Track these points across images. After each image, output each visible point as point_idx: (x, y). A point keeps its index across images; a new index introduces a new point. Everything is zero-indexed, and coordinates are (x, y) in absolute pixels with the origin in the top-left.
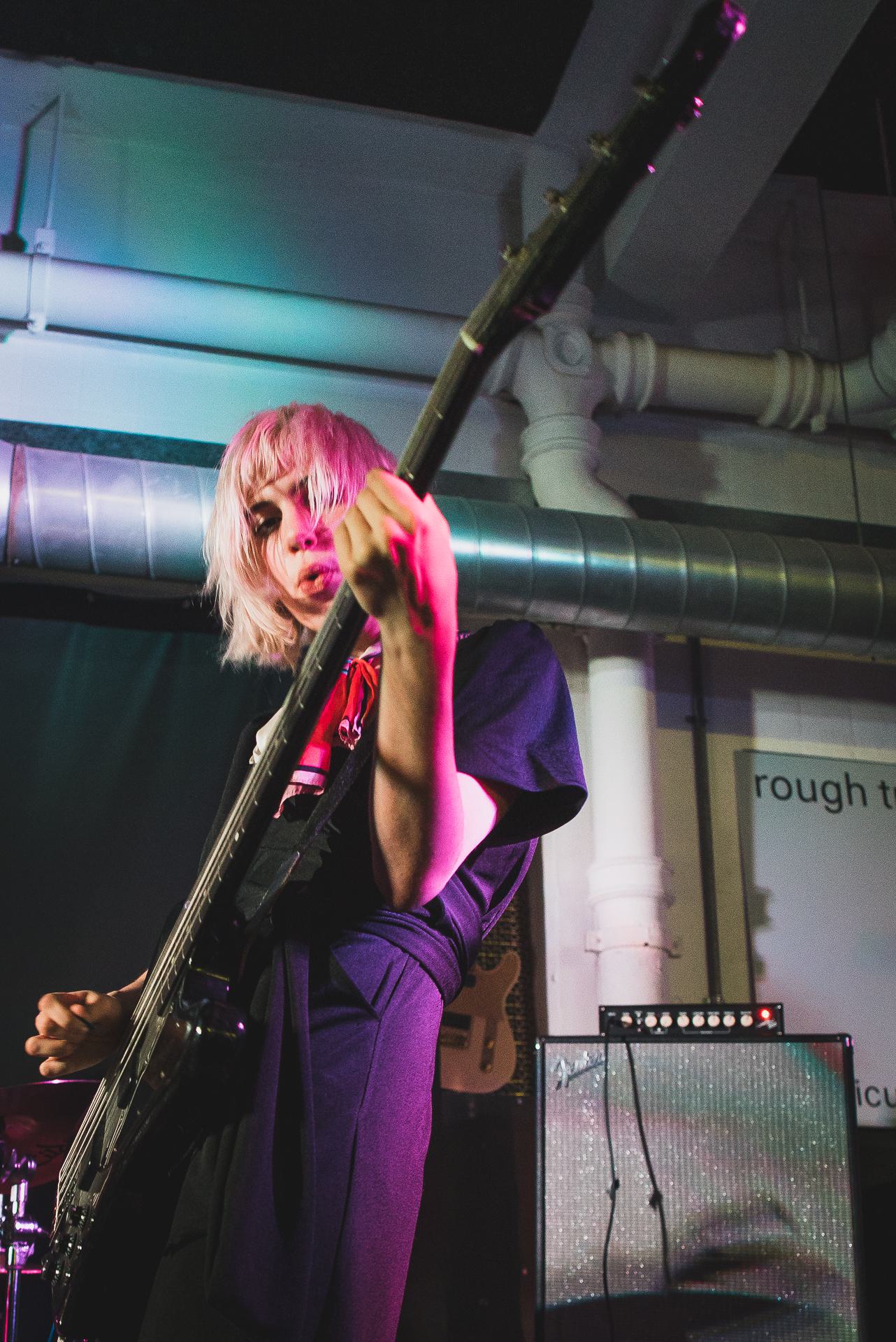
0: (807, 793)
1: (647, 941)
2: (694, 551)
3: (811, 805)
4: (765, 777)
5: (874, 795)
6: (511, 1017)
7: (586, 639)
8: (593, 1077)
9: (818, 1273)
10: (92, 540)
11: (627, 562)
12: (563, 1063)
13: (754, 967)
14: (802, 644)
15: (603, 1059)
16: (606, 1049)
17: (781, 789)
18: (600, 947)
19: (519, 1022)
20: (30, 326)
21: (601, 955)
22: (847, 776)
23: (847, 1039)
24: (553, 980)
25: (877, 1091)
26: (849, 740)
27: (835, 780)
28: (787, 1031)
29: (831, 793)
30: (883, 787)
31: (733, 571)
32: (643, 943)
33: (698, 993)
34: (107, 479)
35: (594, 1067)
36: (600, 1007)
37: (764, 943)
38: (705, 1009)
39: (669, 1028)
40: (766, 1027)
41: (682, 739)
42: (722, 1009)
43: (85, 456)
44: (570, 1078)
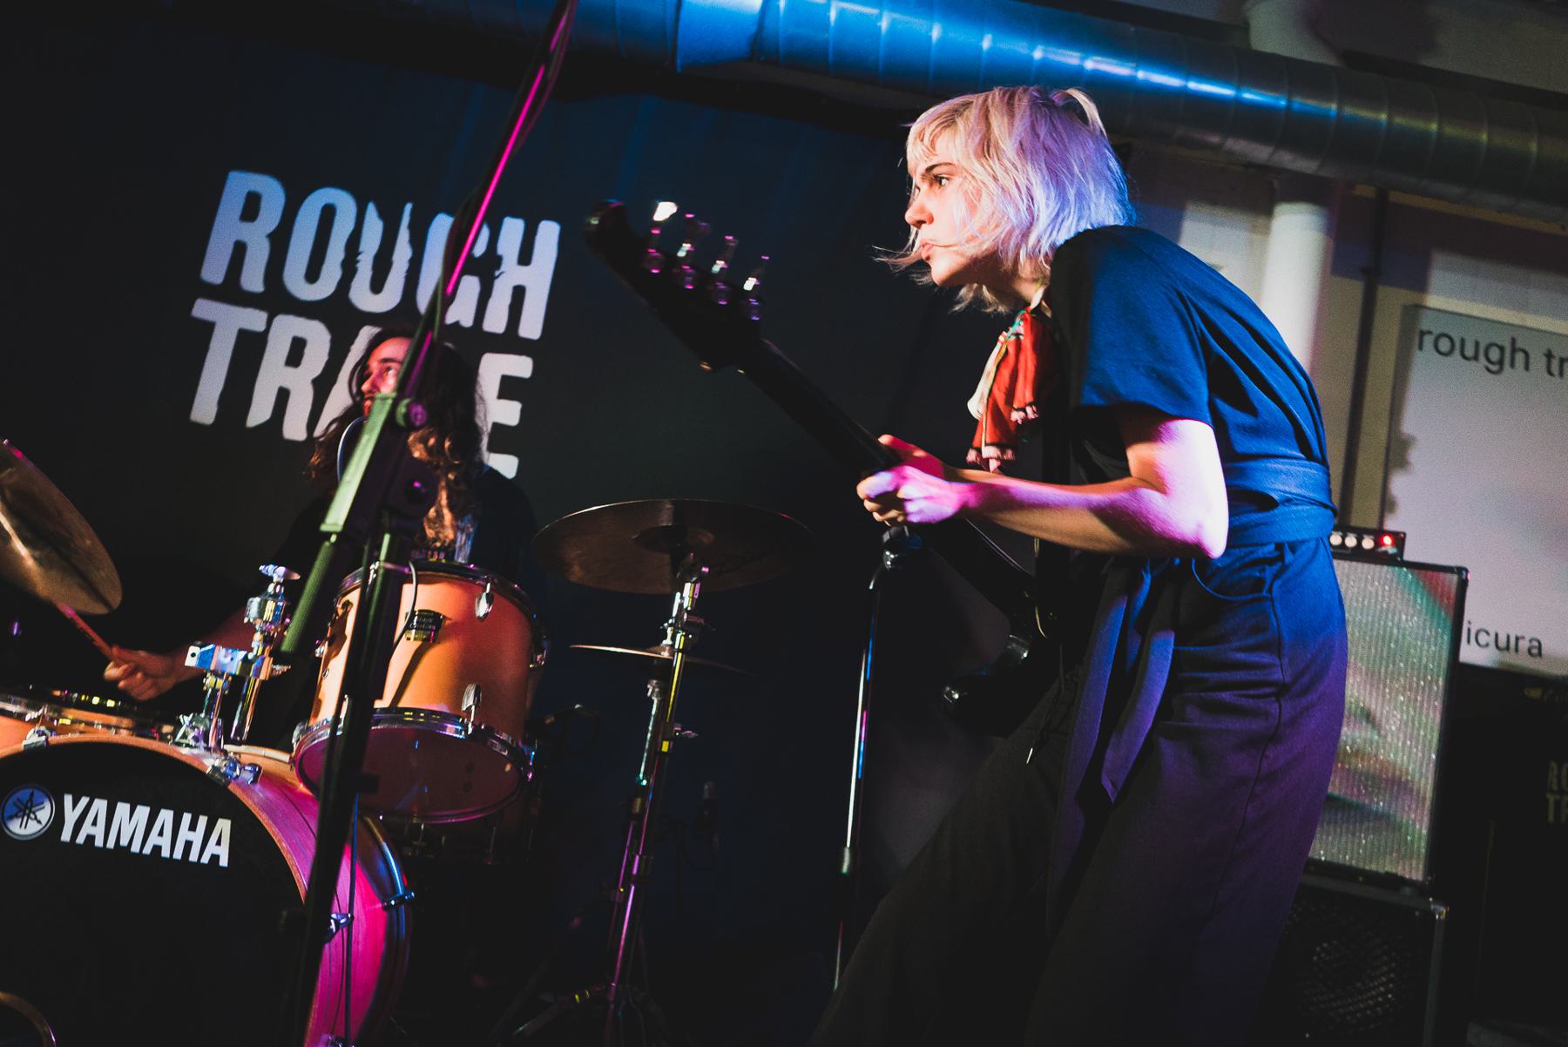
0: (1469, 352)
3: (1473, 363)
4: (1430, 333)
5: (1538, 361)
7: (1276, 183)
9: (1397, 784)
10: (831, 50)
13: (1387, 504)
14: (1491, 208)
17: (1444, 345)
22: (1513, 341)
23: (1464, 573)
25: (1488, 633)
26: (1523, 307)
27: (1500, 343)
28: (1409, 556)
29: (1494, 354)
30: (1549, 355)
31: (1434, 127)
37: (1399, 485)
40: (1386, 552)
41: (1355, 288)
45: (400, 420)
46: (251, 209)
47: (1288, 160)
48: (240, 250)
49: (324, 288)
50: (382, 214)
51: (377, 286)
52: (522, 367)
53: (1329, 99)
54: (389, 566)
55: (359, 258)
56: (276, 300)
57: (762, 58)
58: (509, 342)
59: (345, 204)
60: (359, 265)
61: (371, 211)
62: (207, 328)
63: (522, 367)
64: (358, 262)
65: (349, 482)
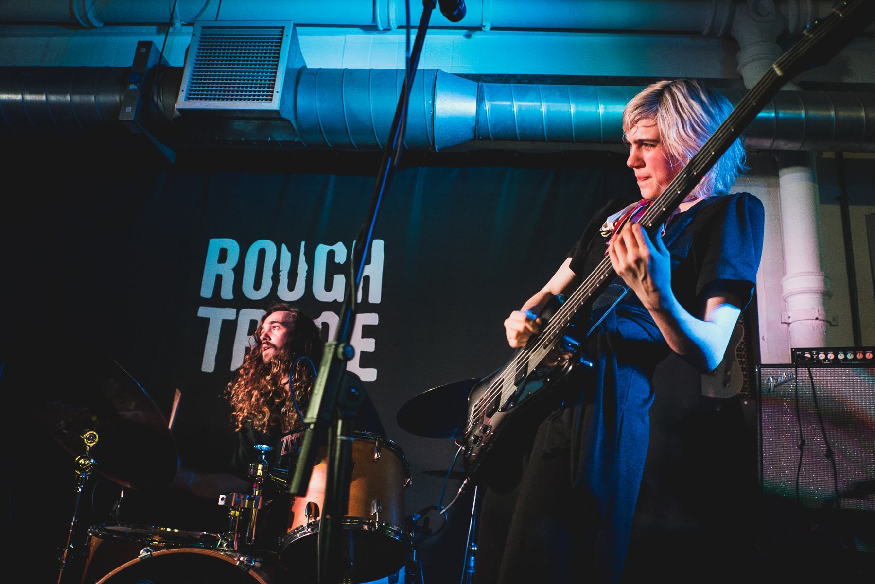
1: (817, 317)
2: (838, 105)
6: (740, 359)
8: (789, 386)
11: (801, 114)
12: (771, 378)
15: (795, 376)
16: (796, 371)
18: (790, 321)
19: (744, 362)
20: (483, 29)
21: (791, 325)
24: (763, 338)
31: (863, 114)
32: (815, 318)
33: (851, 343)
34: (522, 97)
35: (790, 380)
36: (792, 349)
38: (854, 350)
39: (832, 360)
42: (864, 350)
43: (512, 85)
44: (775, 386)
45: (340, 356)
46: (223, 257)
47: (782, 145)
48: (219, 278)
49: (264, 291)
50: (289, 250)
51: (291, 287)
52: (373, 319)
53: (799, 109)
54: (344, 438)
55: (280, 274)
56: (240, 302)
57: (481, 137)
58: (365, 307)
59: (270, 246)
60: (280, 277)
61: (284, 247)
62: (207, 320)
63: (373, 319)
64: (280, 276)
65: (317, 394)
